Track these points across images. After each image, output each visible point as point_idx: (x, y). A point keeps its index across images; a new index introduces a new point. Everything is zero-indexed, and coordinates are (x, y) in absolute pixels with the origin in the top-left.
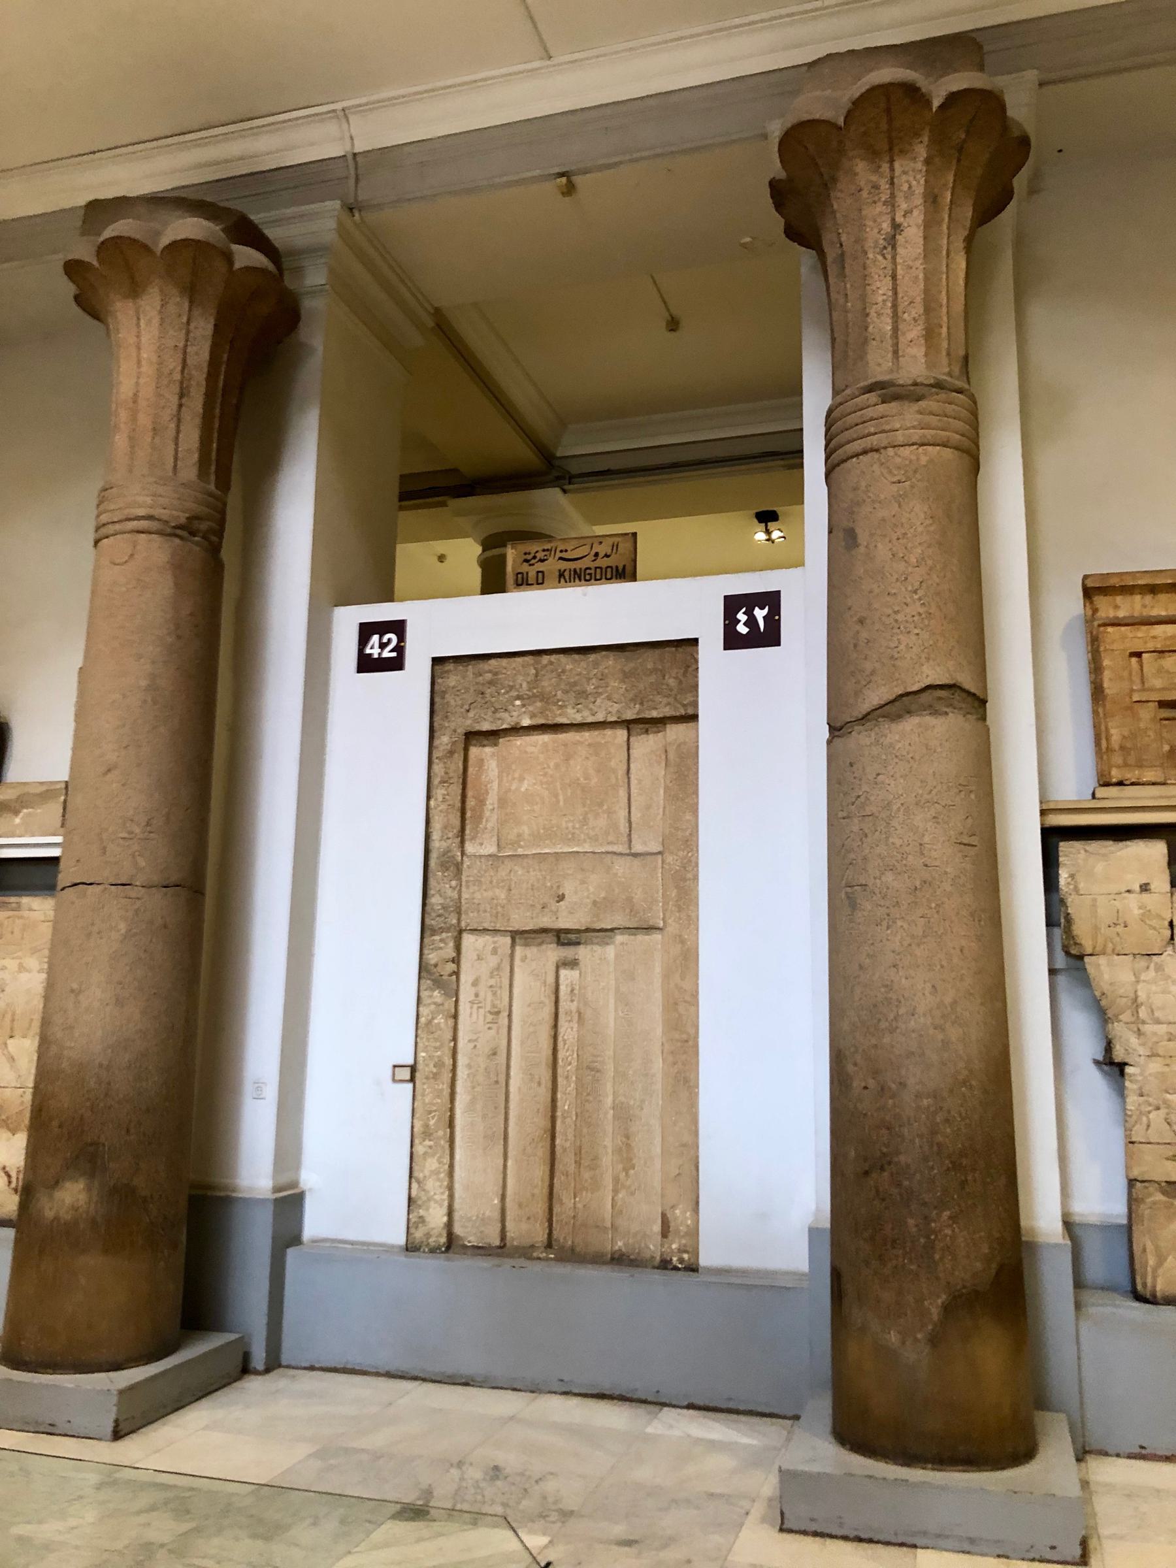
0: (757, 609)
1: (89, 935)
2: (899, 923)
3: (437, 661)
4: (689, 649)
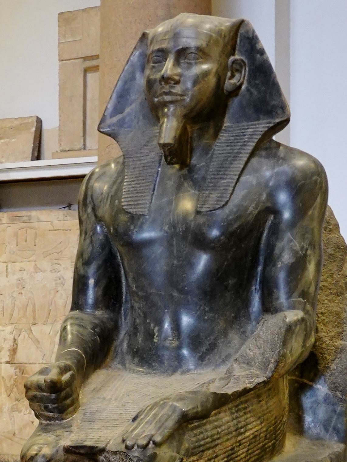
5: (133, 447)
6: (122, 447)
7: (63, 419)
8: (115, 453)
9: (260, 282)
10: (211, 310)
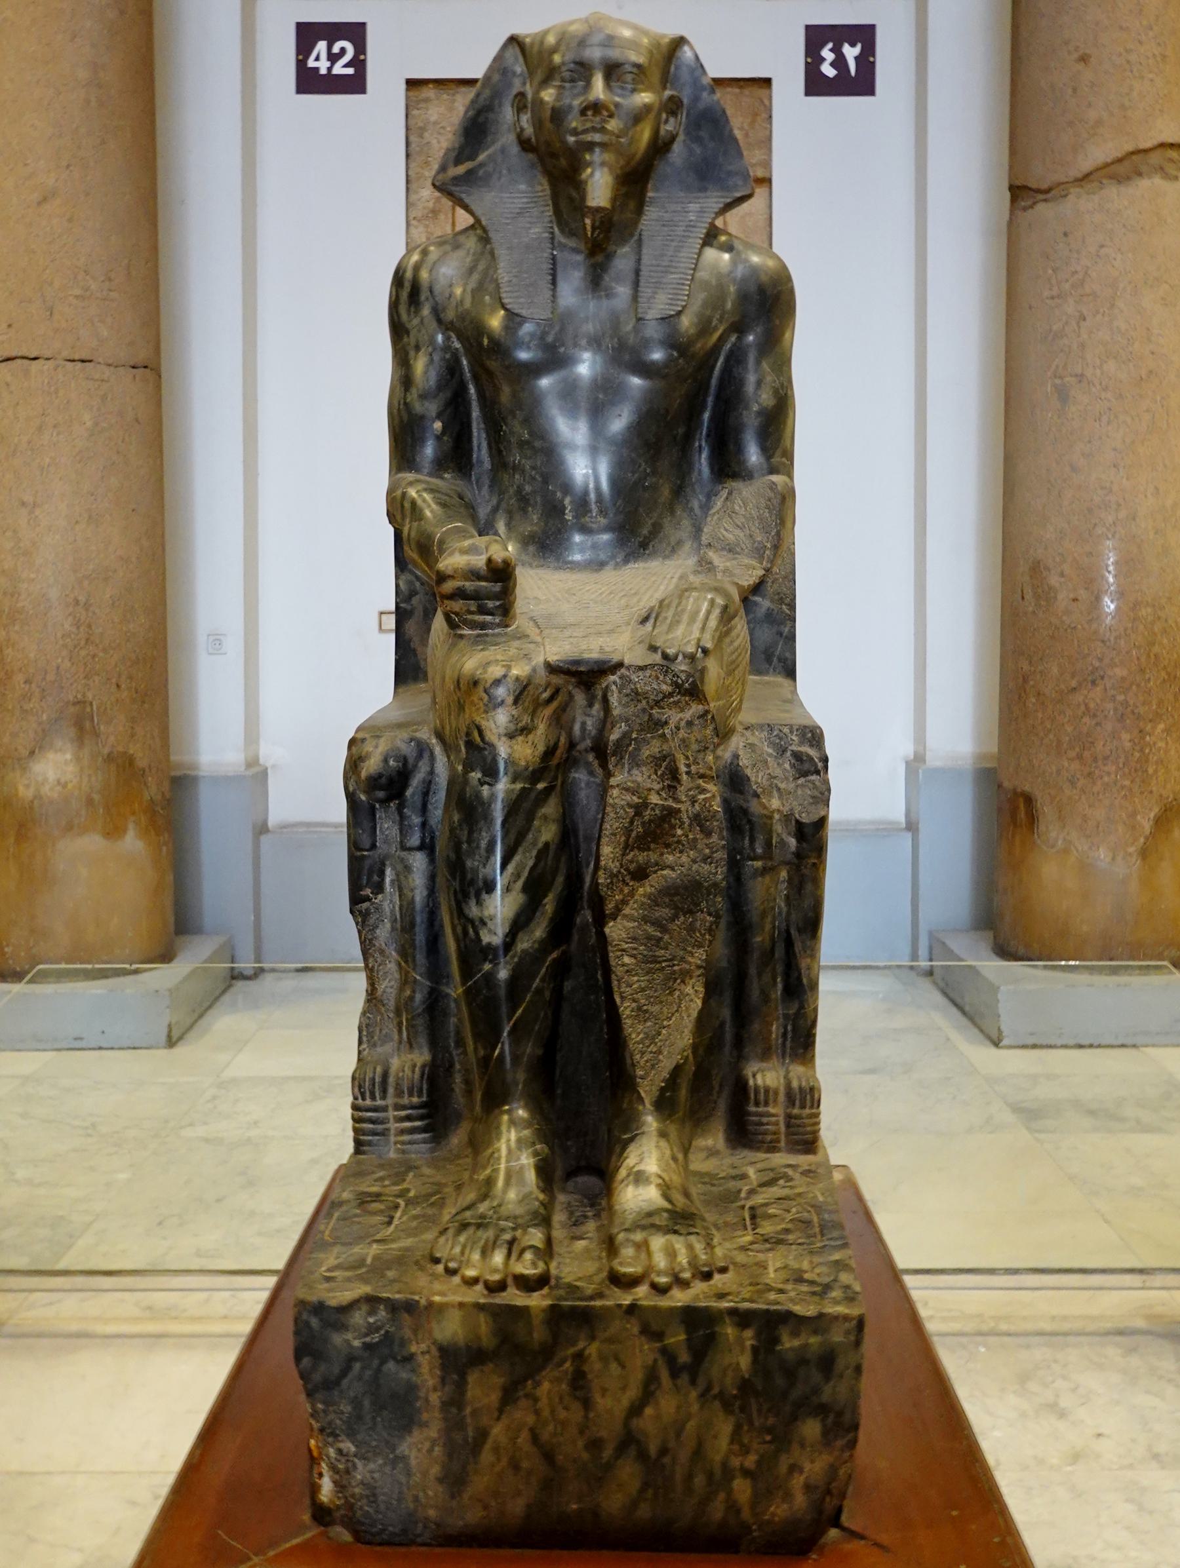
1: (40, 429)
4: (762, 92)
5: (676, 658)
6: (657, 658)
7: (507, 626)
8: (642, 668)
10: (654, 473)
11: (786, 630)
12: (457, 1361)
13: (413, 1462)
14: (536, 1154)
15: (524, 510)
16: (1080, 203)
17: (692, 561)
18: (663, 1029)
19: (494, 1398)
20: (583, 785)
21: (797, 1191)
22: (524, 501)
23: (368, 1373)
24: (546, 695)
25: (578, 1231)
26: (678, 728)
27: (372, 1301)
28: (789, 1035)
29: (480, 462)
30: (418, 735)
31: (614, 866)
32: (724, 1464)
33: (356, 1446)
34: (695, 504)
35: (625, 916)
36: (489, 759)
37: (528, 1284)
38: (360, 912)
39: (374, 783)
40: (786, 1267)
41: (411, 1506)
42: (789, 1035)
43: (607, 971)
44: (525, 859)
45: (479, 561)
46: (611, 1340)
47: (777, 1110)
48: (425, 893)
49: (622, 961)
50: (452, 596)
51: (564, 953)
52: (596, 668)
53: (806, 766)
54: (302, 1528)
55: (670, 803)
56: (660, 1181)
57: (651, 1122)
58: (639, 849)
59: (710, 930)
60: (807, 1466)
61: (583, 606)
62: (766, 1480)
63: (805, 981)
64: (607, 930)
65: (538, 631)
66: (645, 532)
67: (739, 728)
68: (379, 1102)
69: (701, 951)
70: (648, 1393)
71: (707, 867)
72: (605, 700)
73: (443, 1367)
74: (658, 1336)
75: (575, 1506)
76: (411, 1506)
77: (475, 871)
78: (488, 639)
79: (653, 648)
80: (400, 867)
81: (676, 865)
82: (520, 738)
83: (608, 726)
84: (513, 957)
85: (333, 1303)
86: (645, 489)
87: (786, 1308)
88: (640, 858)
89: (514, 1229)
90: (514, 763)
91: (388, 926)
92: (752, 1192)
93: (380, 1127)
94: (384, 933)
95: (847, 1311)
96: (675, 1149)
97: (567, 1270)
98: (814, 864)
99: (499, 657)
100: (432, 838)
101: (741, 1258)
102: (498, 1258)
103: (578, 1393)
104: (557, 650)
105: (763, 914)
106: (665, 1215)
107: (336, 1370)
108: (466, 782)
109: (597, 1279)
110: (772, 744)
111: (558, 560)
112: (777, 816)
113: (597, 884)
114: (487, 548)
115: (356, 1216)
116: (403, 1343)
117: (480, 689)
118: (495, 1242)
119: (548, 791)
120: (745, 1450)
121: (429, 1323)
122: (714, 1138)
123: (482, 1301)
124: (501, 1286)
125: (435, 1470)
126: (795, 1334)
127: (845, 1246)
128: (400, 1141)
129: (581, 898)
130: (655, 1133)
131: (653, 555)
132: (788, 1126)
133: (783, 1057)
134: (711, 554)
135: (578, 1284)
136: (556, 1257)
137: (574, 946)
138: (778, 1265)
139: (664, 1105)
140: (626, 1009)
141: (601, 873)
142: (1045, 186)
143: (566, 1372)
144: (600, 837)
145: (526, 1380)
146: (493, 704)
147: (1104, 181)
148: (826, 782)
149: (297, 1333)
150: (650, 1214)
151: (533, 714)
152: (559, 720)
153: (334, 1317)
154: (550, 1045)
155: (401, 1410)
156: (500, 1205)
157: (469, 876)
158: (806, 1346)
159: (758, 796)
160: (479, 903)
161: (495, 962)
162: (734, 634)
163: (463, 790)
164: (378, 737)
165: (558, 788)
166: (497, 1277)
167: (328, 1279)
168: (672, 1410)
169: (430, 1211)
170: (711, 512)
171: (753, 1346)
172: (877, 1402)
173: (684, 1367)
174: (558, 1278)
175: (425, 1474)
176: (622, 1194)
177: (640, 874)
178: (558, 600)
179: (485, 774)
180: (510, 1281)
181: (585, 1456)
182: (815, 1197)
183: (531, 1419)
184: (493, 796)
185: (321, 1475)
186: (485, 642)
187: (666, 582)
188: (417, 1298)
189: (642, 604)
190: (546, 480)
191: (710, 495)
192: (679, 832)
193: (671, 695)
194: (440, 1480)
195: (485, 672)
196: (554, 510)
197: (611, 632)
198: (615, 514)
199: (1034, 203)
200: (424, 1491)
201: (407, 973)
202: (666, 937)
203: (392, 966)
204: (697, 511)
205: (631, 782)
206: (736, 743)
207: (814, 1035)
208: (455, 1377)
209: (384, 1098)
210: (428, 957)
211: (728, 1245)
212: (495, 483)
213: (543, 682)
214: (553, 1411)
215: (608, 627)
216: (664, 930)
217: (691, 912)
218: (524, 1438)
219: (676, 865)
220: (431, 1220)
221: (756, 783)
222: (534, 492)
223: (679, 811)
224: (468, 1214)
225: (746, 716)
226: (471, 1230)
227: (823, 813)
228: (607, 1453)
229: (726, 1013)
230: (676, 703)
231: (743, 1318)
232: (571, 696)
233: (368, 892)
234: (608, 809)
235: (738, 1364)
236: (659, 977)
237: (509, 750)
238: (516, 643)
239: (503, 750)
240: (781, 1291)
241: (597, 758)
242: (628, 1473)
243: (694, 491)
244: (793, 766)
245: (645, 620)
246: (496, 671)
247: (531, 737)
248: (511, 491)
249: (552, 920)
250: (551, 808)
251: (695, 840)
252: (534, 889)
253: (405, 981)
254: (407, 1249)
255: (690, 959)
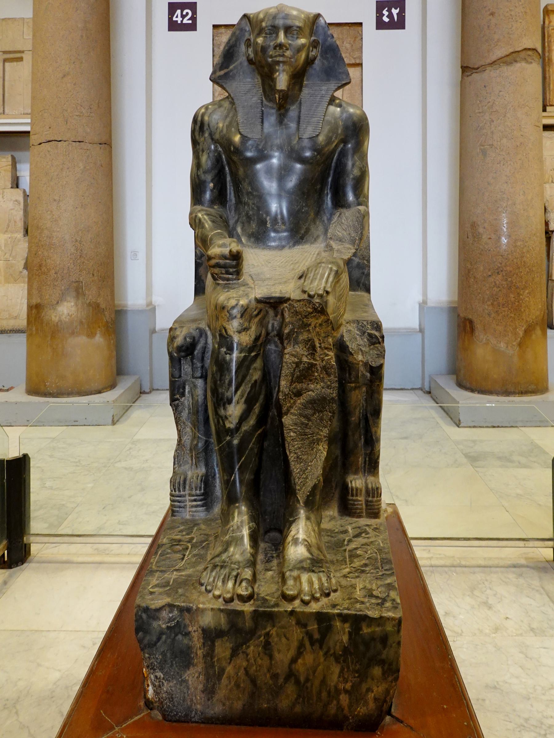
0: (393, 9)
2: (509, 163)
3: (215, 27)
6: (306, 296)
7: (239, 280)
8: (299, 301)
9: (331, 188)
10: (307, 206)
11: (366, 271)
12: (210, 636)
13: (190, 683)
14: (250, 528)
15: (249, 222)
16: (491, 74)
17: (323, 245)
18: (309, 466)
19: (228, 653)
20: (273, 352)
21: (371, 540)
22: (249, 218)
23: (169, 641)
24: (255, 313)
25: (268, 566)
26: (315, 327)
27: (171, 606)
28: (367, 463)
29: (231, 200)
30: (201, 326)
31: (286, 391)
32: (336, 687)
33: (164, 675)
34: (325, 218)
35: (292, 413)
36: (230, 342)
37: (244, 599)
38: (175, 405)
39: (180, 349)
40: (364, 588)
41: (189, 703)
42: (367, 463)
43: (284, 439)
44: (246, 388)
45: (226, 251)
46: (283, 627)
47: (361, 498)
48: (203, 397)
49: (290, 435)
50: (214, 266)
51: (263, 430)
52: (278, 301)
53: (374, 340)
54: (138, 711)
55: (312, 361)
56: (306, 543)
57: (302, 513)
58: (298, 382)
59: (330, 420)
60: (375, 689)
61: (274, 269)
62: (355, 694)
63: (374, 438)
64: (283, 420)
65: (252, 282)
66: (302, 232)
67: (344, 323)
68: (182, 493)
69: (326, 429)
70: (300, 653)
71: (329, 390)
72: (283, 315)
73: (204, 638)
74: (305, 626)
75: (266, 706)
76: (189, 703)
77: (223, 394)
78: (230, 286)
79: (304, 292)
80: (192, 385)
81: (315, 389)
82: (244, 333)
83: (284, 326)
84: (240, 434)
85: (153, 607)
86: (303, 213)
87: (364, 613)
88: (298, 386)
89: (238, 569)
90: (240, 344)
91: (187, 411)
92: (350, 541)
93: (182, 504)
94: (185, 414)
95: (393, 615)
96: (314, 525)
97: (262, 589)
98: (378, 385)
99: (235, 295)
100: (206, 373)
101: (344, 582)
102: (230, 584)
103: (267, 652)
104: (260, 292)
105: (355, 408)
106: (308, 561)
107: (154, 639)
108: (219, 352)
109: (276, 595)
110: (359, 330)
111: (264, 245)
112: (361, 363)
113: (279, 399)
114: (230, 244)
115: (168, 553)
116: (185, 626)
117: (226, 310)
118: (229, 577)
119: (256, 356)
120: (346, 681)
121: (197, 617)
122: (332, 511)
123: (222, 607)
124: (231, 600)
125: (201, 687)
126: (369, 626)
127: (392, 574)
128: (192, 511)
129: (272, 404)
130: (304, 518)
131: (306, 242)
132: (367, 505)
133: (365, 473)
134: (331, 242)
135: (266, 597)
136: (258, 581)
137: (268, 426)
138: (361, 586)
139: (309, 504)
140: (292, 457)
141: (280, 394)
142: (476, 67)
143: (262, 641)
144: (280, 377)
145: (242, 646)
146: (231, 318)
147: (501, 64)
148: (383, 347)
149: (136, 621)
150: (301, 561)
151: (250, 322)
152: (262, 323)
153: (152, 614)
154: (257, 474)
155: (184, 658)
156: (232, 556)
157: (220, 396)
158: (374, 632)
159: (352, 355)
160: (225, 409)
161: (232, 436)
162: (341, 281)
163: (218, 357)
164: (182, 327)
165: (261, 354)
166: (228, 596)
167: (151, 593)
168: (311, 661)
169: (202, 552)
170: (333, 222)
171: (349, 631)
172: (409, 653)
173: (317, 640)
174: (258, 594)
175: (196, 689)
176: (289, 550)
177: (298, 394)
178: (263, 265)
179: (228, 349)
180: (235, 597)
181: (271, 682)
182: (379, 544)
183: (245, 664)
184: (231, 360)
185: (148, 686)
186: (229, 288)
187: (311, 256)
188: (191, 605)
189: (300, 268)
190: (259, 209)
191: (332, 215)
192: (316, 374)
193: (312, 313)
194: (203, 692)
195: (228, 303)
196: (262, 223)
197: (285, 282)
198: (290, 224)
199: (472, 74)
200: (195, 696)
201: (195, 433)
202: (310, 423)
203: (188, 429)
204: (326, 221)
205: (294, 353)
206: (343, 330)
207: (379, 462)
208: (209, 643)
209: (184, 491)
210: (204, 427)
211: (338, 574)
212: (237, 209)
213: (254, 307)
214: (255, 661)
215: (284, 280)
216: (309, 420)
217: (321, 411)
218: (242, 672)
219: (315, 389)
220: (202, 557)
221: (352, 348)
222: (254, 214)
223: (316, 364)
224: (217, 559)
225: (348, 316)
226: (218, 569)
227: (382, 362)
228: (281, 680)
229: (338, 452)
230: (314, 316)
231: (344, 618)
232: (267, 312)
233: (178, 396)
234: (284, 364)
235: (342, 640)
236: (307, 442)
237: (238, 339)
238: (242, 288)
239: (236, 338)
240: (363, 603)
241: (279, 339)
242: (291, 689)
243: (325, 213)
244: (368, 340)
245: (300, 278)
246: (233, 302)
247: (248, 332)
248: (244, 213)
249: (258, 416)
250: (258, 364)
251: (323, 378)
252: (250, 402)
253: (194, 437)
254: (189, 576)
255: (321, 433)
